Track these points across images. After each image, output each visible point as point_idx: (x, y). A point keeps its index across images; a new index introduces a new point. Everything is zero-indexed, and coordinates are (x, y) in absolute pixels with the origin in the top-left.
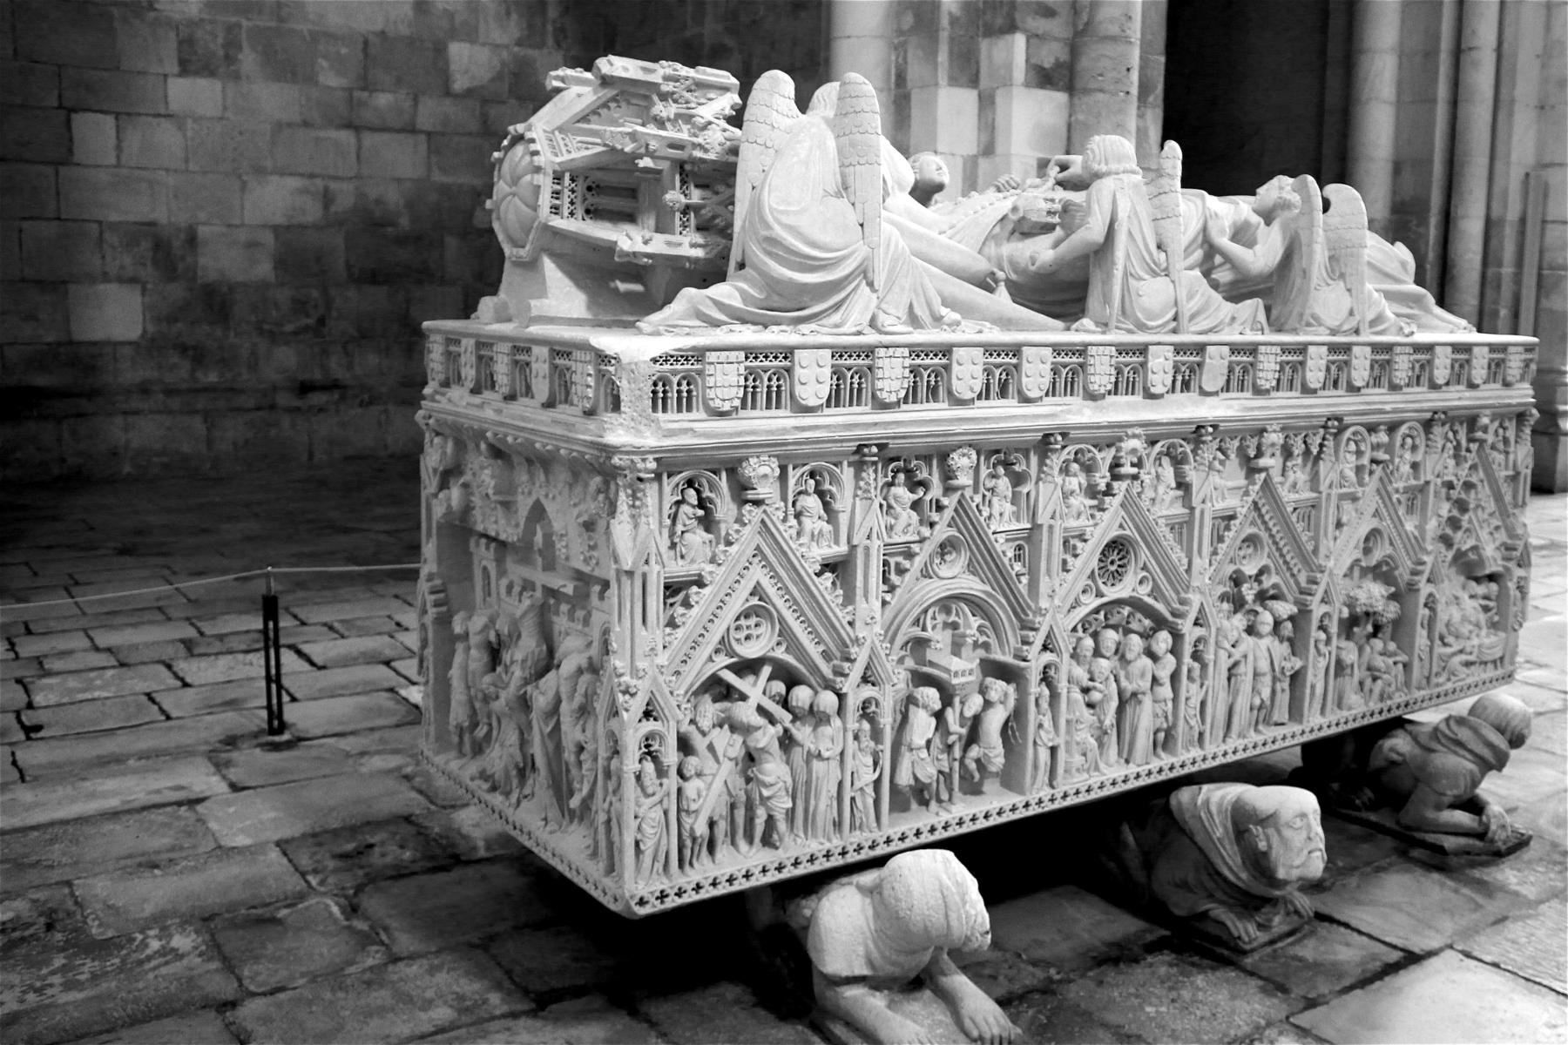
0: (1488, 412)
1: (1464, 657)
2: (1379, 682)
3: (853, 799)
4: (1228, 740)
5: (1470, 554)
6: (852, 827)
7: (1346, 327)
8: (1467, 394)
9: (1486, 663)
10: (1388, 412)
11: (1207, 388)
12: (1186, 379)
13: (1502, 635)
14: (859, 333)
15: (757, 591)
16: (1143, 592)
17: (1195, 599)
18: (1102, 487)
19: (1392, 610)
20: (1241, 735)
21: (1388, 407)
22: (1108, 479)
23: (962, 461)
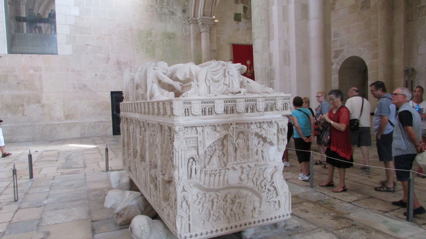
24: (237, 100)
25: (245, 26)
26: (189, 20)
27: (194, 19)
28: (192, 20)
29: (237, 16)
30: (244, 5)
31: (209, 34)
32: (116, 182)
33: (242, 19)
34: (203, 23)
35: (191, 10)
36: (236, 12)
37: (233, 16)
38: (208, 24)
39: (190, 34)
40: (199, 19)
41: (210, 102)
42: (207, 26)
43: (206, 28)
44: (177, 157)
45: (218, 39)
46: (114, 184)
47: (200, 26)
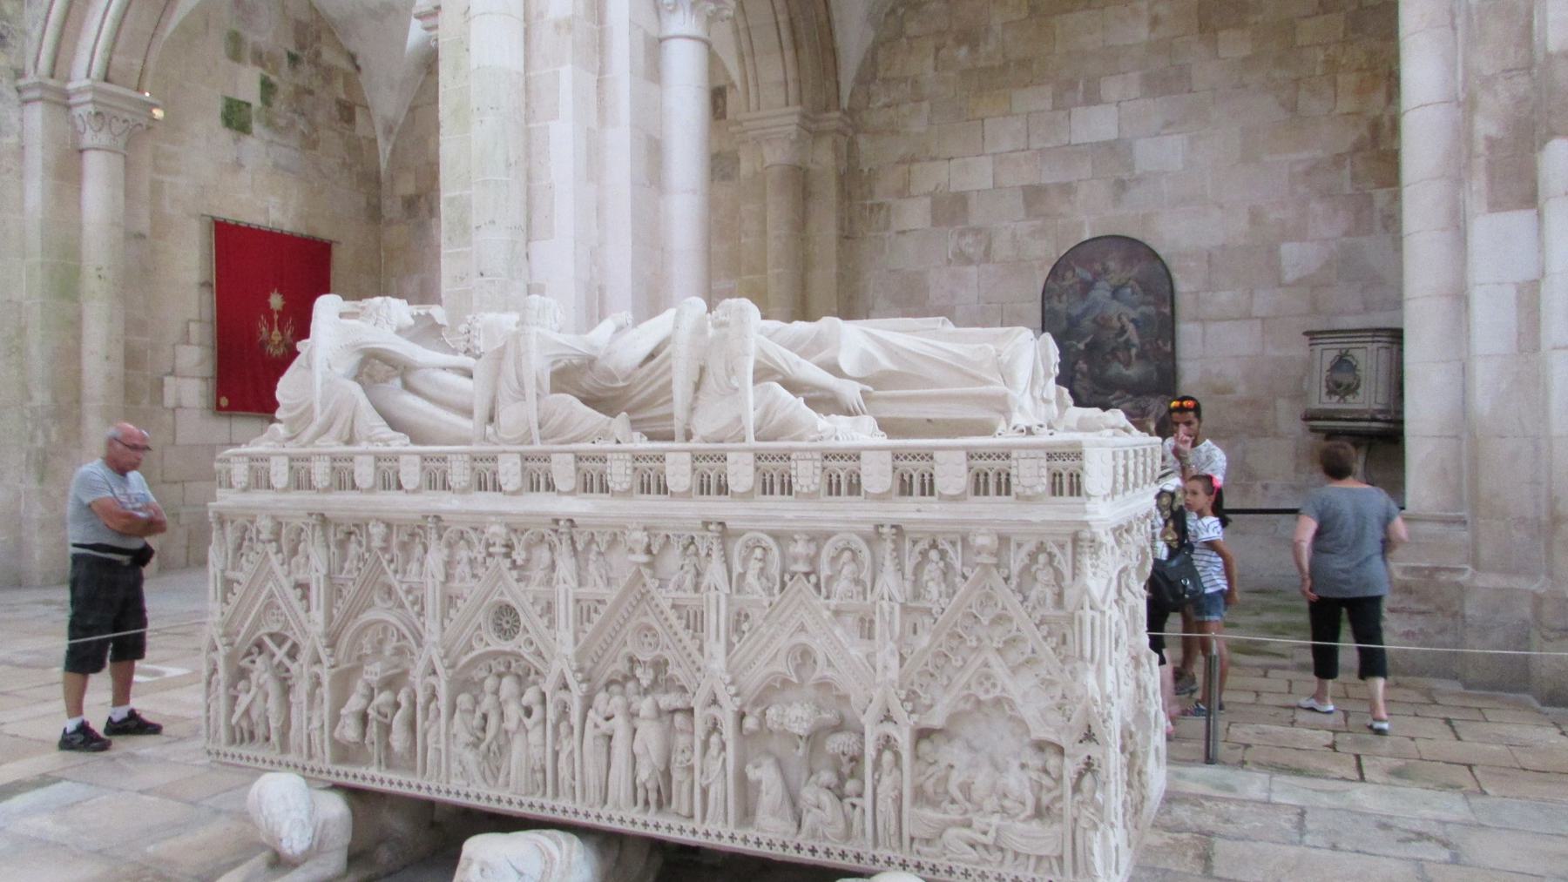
0: (983, 529)
1: (966, 832)
2: (810, 815)
3: (309, 736)
4: (607, 807)
5: (1006, 707)
6: (310, 756)
7: (729, 435)
8: (937, 506)
9: (1028, 857)
10: (791, 520)
11: (561, 489)
12: (536, 480)
13: (1056, 827)
14: (303, 446)
15: (271, 595)
16: (526, 652)
17: (556, 666)
18: (480, 558)
19: (838, 743)
20: (617, 806)
21: (789, 515)
22: (484, 554)
23: (377, 531)
24: (937, 455)
25: (268, 154)
26: (21, 82)
27: (51, 82)
28: (41, 86)
29: (235, 109)
30: (266, 73)
31: (120, 160)
32: (302, 821)
33: (256, 127)
34: (100, 109)
35: (35, 45)
36: (231, 95)
37: (218, 107)
38: (125, 121)
39: (23, 147)
40: (79, 91)
41: (766, 458)
42: (118, 126)
43: (112, 133)
44: (1098, 629)
45: (156, 189)
46: (296, 835)
47: (79, 122)
